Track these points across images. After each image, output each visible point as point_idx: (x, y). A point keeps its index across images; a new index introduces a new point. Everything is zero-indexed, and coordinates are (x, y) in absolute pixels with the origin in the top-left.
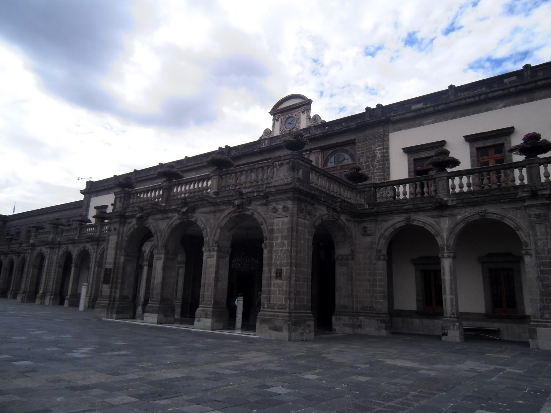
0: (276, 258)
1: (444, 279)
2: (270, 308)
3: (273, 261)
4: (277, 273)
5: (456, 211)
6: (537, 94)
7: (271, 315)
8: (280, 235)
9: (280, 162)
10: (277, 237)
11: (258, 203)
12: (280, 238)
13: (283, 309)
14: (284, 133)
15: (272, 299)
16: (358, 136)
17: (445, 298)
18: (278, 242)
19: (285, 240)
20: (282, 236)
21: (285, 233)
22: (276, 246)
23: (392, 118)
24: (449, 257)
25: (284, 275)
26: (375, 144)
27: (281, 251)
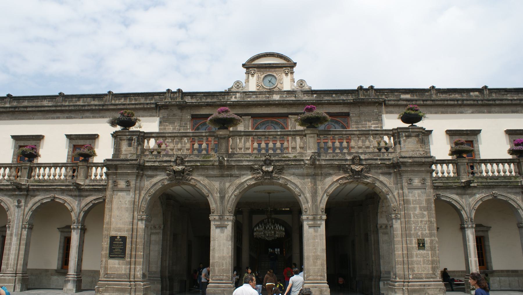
0: (415, 229)
1: (469, 245)
2: (417, 278)
3: (412, 232)
4: (419, 244)
5: (475, 191)
6: (493, 109)
7: (420, 285)
8: (418, 206)
9: (407, 134)
10: (415, 208)
11: (380, 171)
12: (418, 209)
13: (432, 278)
14: (262, 90)
15: (416, 269)
16: (353, 112)
17: (471, 260)
18: (416, 212)
19: (425, 211)
20: (420, 207)
21: (424, 204)
22: (414, 217)
23: (387, 102)
24: (472, 227)
25: (427, 245)
26: (370, 121)
27: (421, 221)
